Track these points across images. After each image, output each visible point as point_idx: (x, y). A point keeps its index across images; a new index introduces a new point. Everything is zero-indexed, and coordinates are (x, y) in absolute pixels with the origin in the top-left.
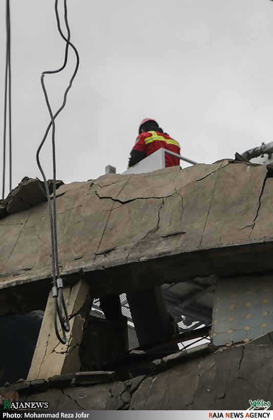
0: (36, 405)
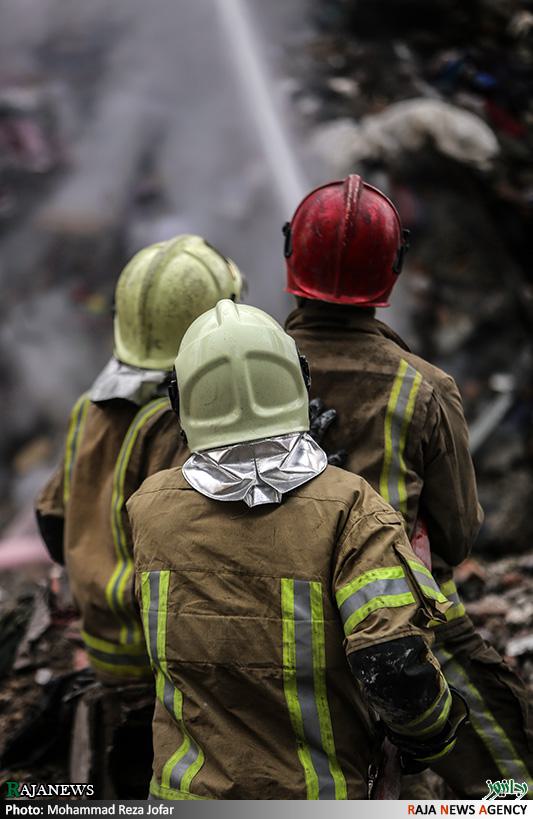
0: (69, 790)
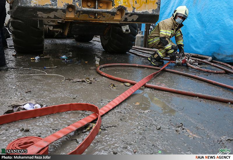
0: (20, 151)
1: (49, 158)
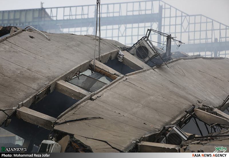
0: (20, 149)
1: (48, 156)
